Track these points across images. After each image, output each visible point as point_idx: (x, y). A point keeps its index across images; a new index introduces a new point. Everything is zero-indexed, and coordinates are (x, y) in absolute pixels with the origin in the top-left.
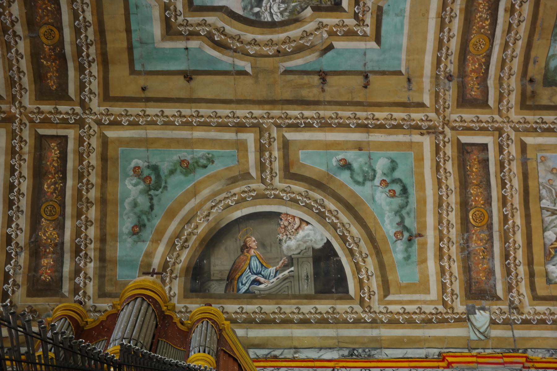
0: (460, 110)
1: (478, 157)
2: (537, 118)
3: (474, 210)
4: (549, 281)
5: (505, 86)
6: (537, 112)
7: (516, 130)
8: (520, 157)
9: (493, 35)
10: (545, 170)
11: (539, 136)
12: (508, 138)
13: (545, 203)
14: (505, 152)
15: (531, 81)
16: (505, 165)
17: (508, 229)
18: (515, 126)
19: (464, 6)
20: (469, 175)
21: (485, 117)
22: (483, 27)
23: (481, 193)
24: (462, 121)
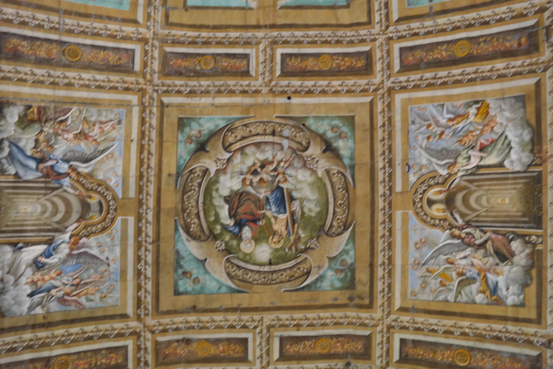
0: (373, 358)
1: (411, 348)
2: (380, 296)
3: (456, 360)
4: (522, 305)
5: (354, 321)
6: (375, 295)
7: (389, 314)
8: (411, 314)
9: (316, 337)
10: (423, 293)
11: (394, 295)
12: (395, 320)
13: (451, 297)
14: (407, 325)
15: (351, 299)
16: (418, 326)
17: (473, 333)
18: (386, 314)
19: (295, 362)
20: (426, 359)
21: (378, 338)
22: (310, 345)
23: (441, 351)
24: (381, 356)
